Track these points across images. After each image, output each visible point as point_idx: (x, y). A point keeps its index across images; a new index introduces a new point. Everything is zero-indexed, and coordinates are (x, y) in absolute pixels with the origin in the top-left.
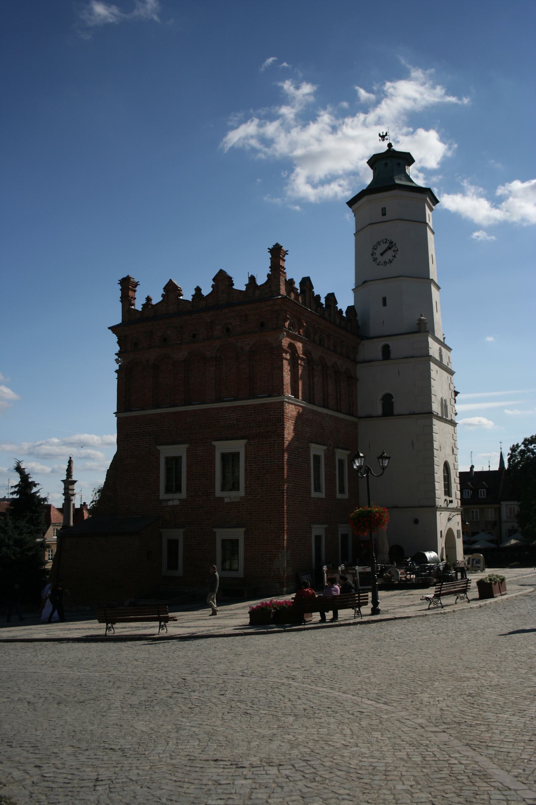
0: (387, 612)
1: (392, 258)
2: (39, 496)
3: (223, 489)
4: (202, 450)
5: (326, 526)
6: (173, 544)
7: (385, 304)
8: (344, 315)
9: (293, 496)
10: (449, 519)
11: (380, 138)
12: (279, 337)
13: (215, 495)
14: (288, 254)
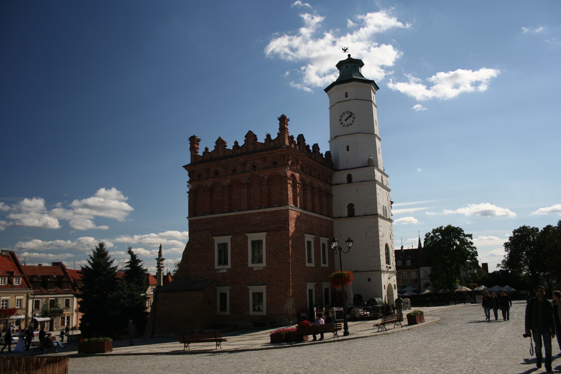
0: (353, 334)
1: (352, 122)
2: (143, 268)
3: (253, 262)
4: (240, 239)
5: (315, 284)
6: (223, 296)
7: (348, 150)
8: (324, 156)
9: (295, 266)
10: (389, 278)
11: (343, 51)
12: (285, 171)
13: (248, 266)
14: (289, 121)
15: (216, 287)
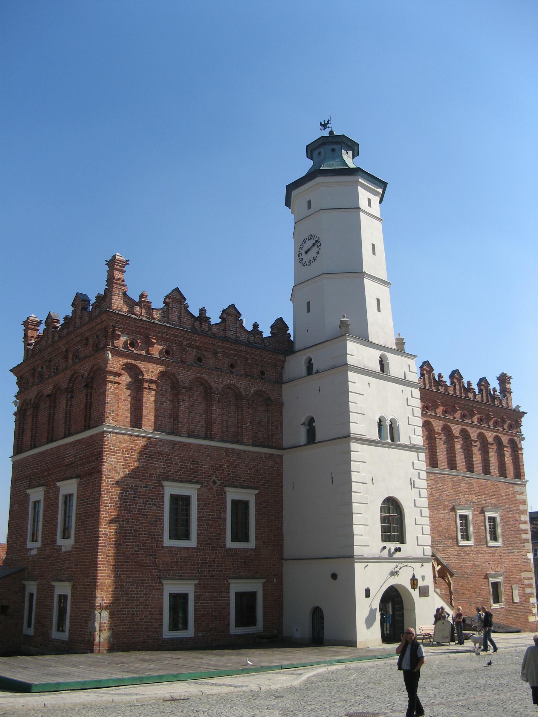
1: (315, 255)
7: (309, 311)
14: (128, 264)
15: (25, 582)
